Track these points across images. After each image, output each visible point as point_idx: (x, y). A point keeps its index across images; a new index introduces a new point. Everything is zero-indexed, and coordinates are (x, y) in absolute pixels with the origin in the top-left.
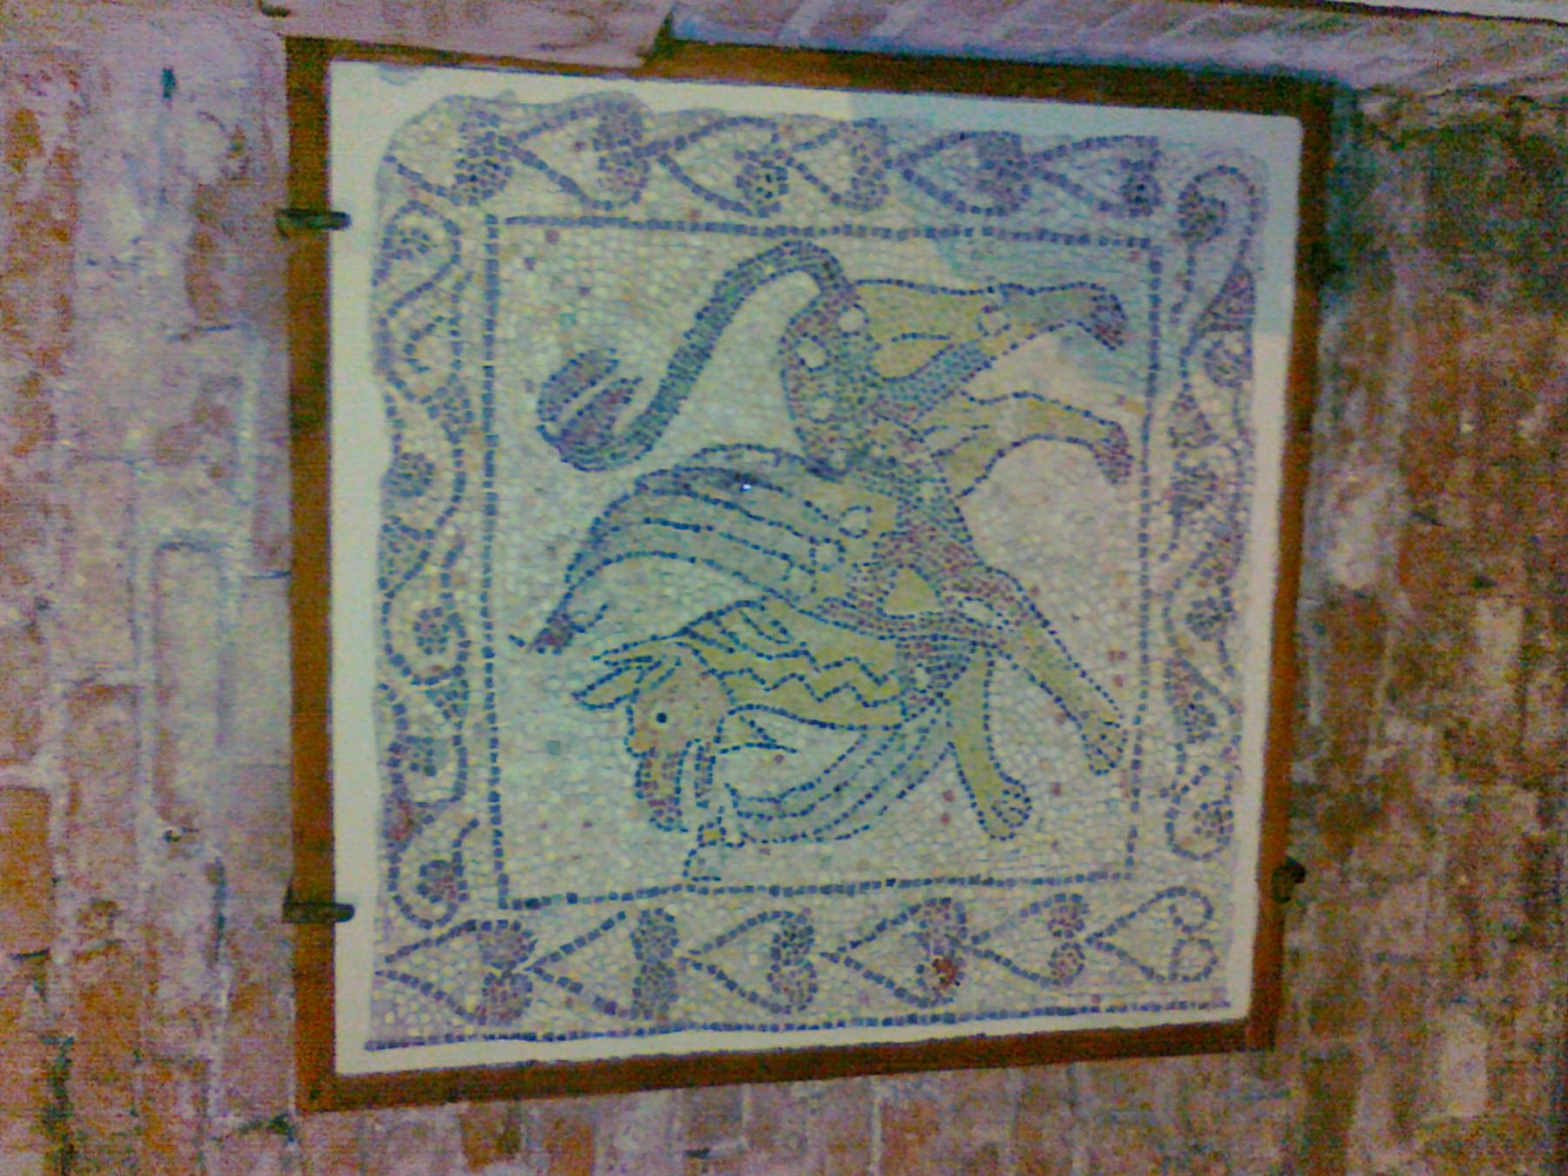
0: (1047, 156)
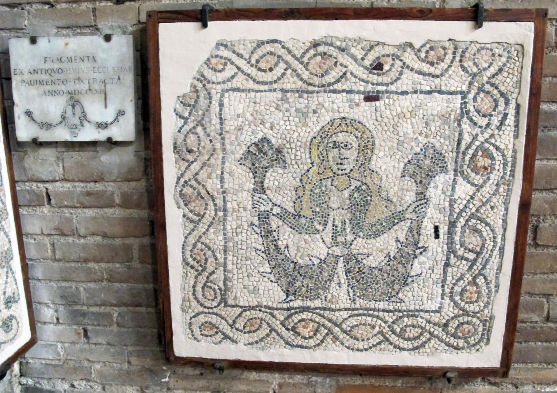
0: (11, 269)
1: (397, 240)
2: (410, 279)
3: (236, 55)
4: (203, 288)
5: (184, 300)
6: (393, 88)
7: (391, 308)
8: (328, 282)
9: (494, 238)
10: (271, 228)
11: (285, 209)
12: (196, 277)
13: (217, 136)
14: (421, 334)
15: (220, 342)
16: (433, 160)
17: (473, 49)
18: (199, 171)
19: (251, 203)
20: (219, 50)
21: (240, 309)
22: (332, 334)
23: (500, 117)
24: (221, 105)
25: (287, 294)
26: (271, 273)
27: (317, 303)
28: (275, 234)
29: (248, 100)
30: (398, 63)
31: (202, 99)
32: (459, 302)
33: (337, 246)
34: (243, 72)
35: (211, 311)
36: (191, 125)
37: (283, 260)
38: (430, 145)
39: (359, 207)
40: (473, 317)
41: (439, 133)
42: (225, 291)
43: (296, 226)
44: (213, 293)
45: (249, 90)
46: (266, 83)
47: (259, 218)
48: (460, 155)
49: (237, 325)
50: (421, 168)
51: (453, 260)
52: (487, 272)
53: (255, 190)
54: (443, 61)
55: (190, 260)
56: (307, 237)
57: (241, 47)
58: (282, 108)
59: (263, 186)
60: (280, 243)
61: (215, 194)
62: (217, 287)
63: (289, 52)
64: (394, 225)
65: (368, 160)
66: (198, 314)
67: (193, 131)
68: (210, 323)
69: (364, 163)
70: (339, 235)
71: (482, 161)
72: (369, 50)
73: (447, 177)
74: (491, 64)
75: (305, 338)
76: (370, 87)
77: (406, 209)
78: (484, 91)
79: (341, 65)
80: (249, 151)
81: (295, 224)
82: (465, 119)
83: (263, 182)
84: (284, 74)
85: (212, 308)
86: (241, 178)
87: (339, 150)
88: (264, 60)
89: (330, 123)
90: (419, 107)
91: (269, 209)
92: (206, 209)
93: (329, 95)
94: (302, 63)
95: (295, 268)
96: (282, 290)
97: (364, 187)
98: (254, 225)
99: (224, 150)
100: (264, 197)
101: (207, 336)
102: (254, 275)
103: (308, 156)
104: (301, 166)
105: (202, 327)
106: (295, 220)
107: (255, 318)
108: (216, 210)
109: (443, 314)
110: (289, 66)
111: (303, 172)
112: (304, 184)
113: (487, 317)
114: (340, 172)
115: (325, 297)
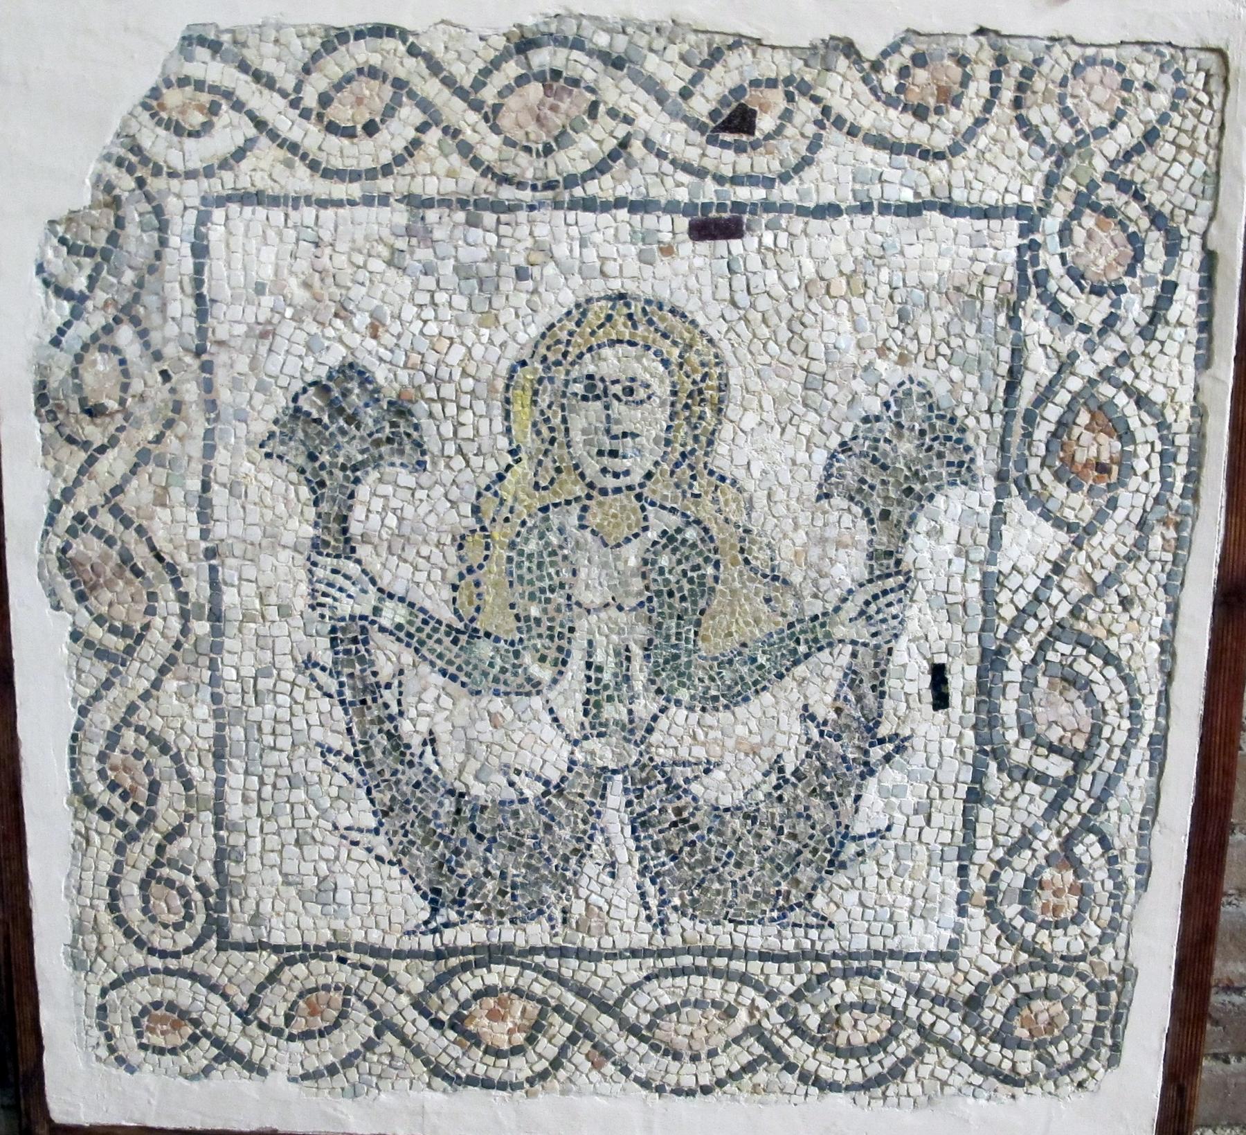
1: (807, 715)
2: (851, 848)
3: (249, 78)
4: (144, 885)
5: (78, 929)
6: (787, 193)
7: (789, 945)
8: (573, 860)
9: (1134, 704)
10: (375, 674)
11: (422, 610)
12: (120, 849)
13: (188, 359)
14: (892, 1034)
15: (206, 1071)
17: (1059, 63)
18: (126, 480)
19: (304, 588)
20: (189, 58)
21: (274, 957)
22: (590, 1036)
23: (1151, 293)
24: (200, 250)
25: (433, 901)
27: (537, 933)
28: (389, 696)
29: (291, 234)
30: (806, 109)
31: (132, 229)
32: (1018, 922)
33: (600, 735)
34: (273, 135)
35: (173, 964)
36: (98, 320)
37: (417, 785)
38: (915, 388)
41: (944, 349)
42: (220, 894)
43: (459, 669)
44: (178, 902)
45: (296, 200)
46: (355, 176)
48: (1018, 424)
49: (265, 1013)
50: (884, 467)
51: (995, 781)
52: (1109, 820)
53: (318, 545)
54: (956, 103)
56: (498, 704)
57: (269, 48)
58: (408, 261)
59: (345, 531)
60: (406, 726)
61: (182, 558)
62: (191, 883)
63: (435, 67)
64: (796, 663)
65: (703, 439)
66: (130, 975)
67: (104, 340)
68: (172, 1006)
69: (693, 451)
70: (610, 699)
71: (1092, 446)
72: (708, 64)
73: (973, 498)
74: (1119, 116)
76: (709, 191)
77: (837, 609)
78: (1095, 207)
79: (613, 113)
80: (297, 410)
81: (458, 661)
82: (1032, 303)
83: (345, 519)
84: (416, 143)
85: (176, 955)
86: (269, 504)
87: (607, 407)
88: (345, 94)
90: (878, 258)
91: (367, 611)
92: (150, 611)
93: (571, 216)
94: (476, 106)
95: (458, 811)
96: (417, 888)
97: (691, 534)
98: (316, 665)
99: (211, 405)
100: (351, 568)
101: (161, 1051)
102: (319, 837)
103: (499, 426)
104: (476, 462)
105: (145, 1021)
106: (456, 649)
107: (326, 988)
108: (184, 616)
109: (964, 964)
110: (431, 117)
111: (484, 481)
112: (487, 523)
113: (1111, 972)
114: (610, 482)
115: (564, 911)
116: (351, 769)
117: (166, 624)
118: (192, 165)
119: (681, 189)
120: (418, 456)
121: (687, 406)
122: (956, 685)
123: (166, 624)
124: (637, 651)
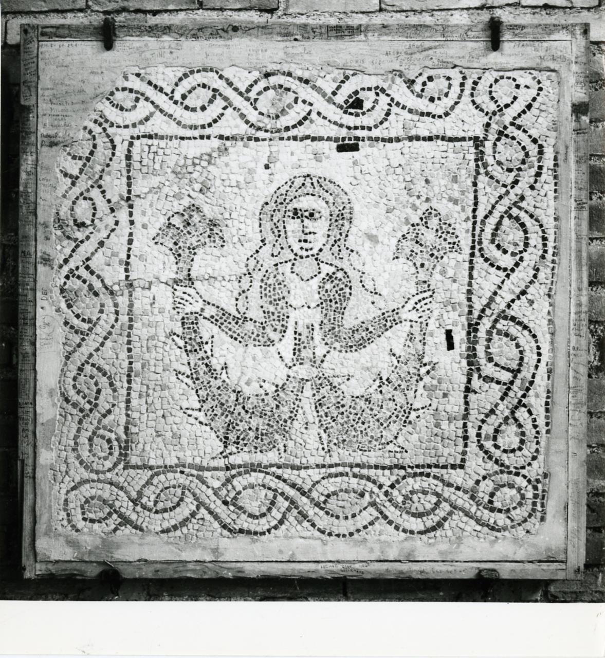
2: (413, 415)
3: (152, 88)
4: (90, 439)
8: (289, 421)
10: (201, 338)
11: (222, 309)
12: (80, 422)
13: (123, 203)
14: (437, 504)
16: (439, 234)
17: (489, 78)
19: (171, 300)
22: (297, 508)
25: (225, 442)
26: (200, 410)
30: (384, 100)
31: (100, 148)
32: (492, 450)
33: (301, 364)
34: (161, 111)
37: (219, 388)
38: (433, 212)
39: (333, 303)
40: (517, 474)
42: (127, 442)
44: (106, 446)
45: (171, 137)
47: (183, 324)
49: (144, 500)
50: (421, 245)
51: (476, 383)
52: (531, 400)
55: (72, 393)
63: (230, 84)
64: (387, 330)
65: (344, 235)
67: (86, 194)
68: (100, 498)
69: (339, 240)
72: (343, 82)
75: (256, 517)
76: (344, 132)
79: (304, 102)
80: (170, 224)
86: (155, 263)
87: (302, 221)
89: (289, 183)
91: (198, 310)
92: (101, 312)
94: (248, 99)
95: (237, 400)
96: (218, 437)
97: (340, 275)
98: (175, 334)
100: (191, 291)
105: (86, 506)
106: (237, 326)
107: (174, 487)
109: (468, 470)
110: (229, 104)
112: (251, 271)
113: (538, 475)
114: (304, 253)
115: (285, 446)
116: (189, 381)
117: (109, 317)
118: (126, 123)
119: (334, 131)
120: (221, 243)
121: (336, 221)
122: (457, 339)
123: (109, 317)
124: (317, 327)
